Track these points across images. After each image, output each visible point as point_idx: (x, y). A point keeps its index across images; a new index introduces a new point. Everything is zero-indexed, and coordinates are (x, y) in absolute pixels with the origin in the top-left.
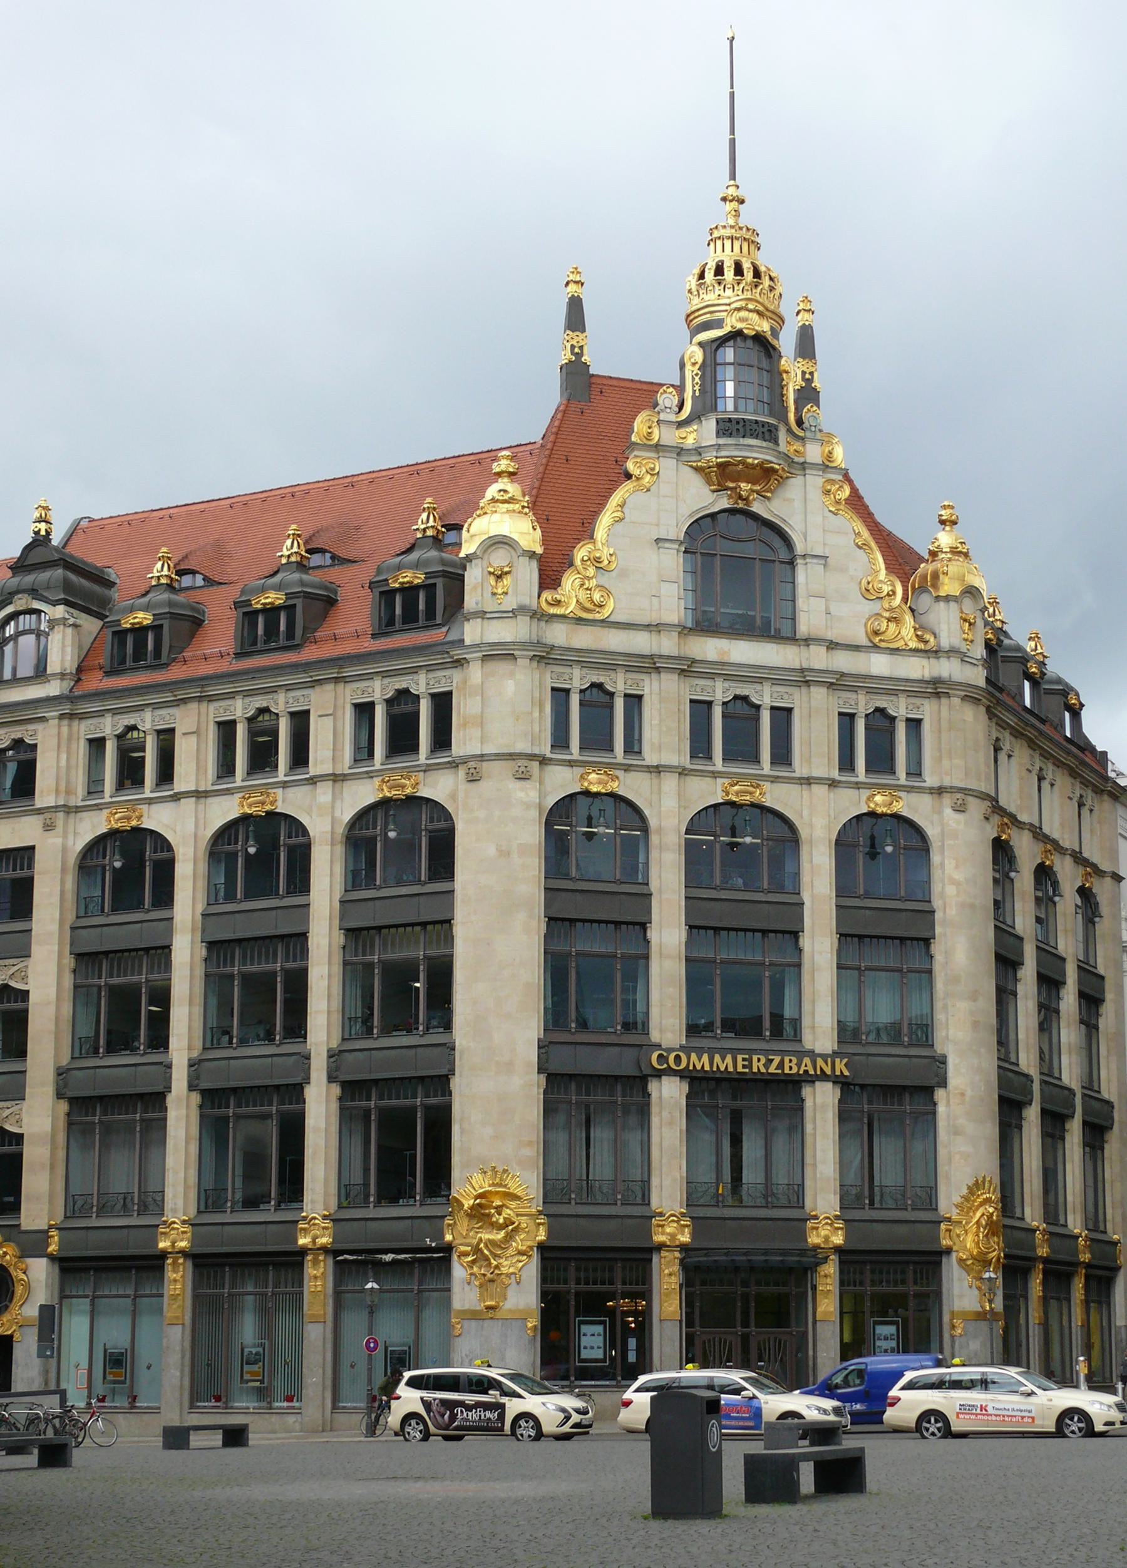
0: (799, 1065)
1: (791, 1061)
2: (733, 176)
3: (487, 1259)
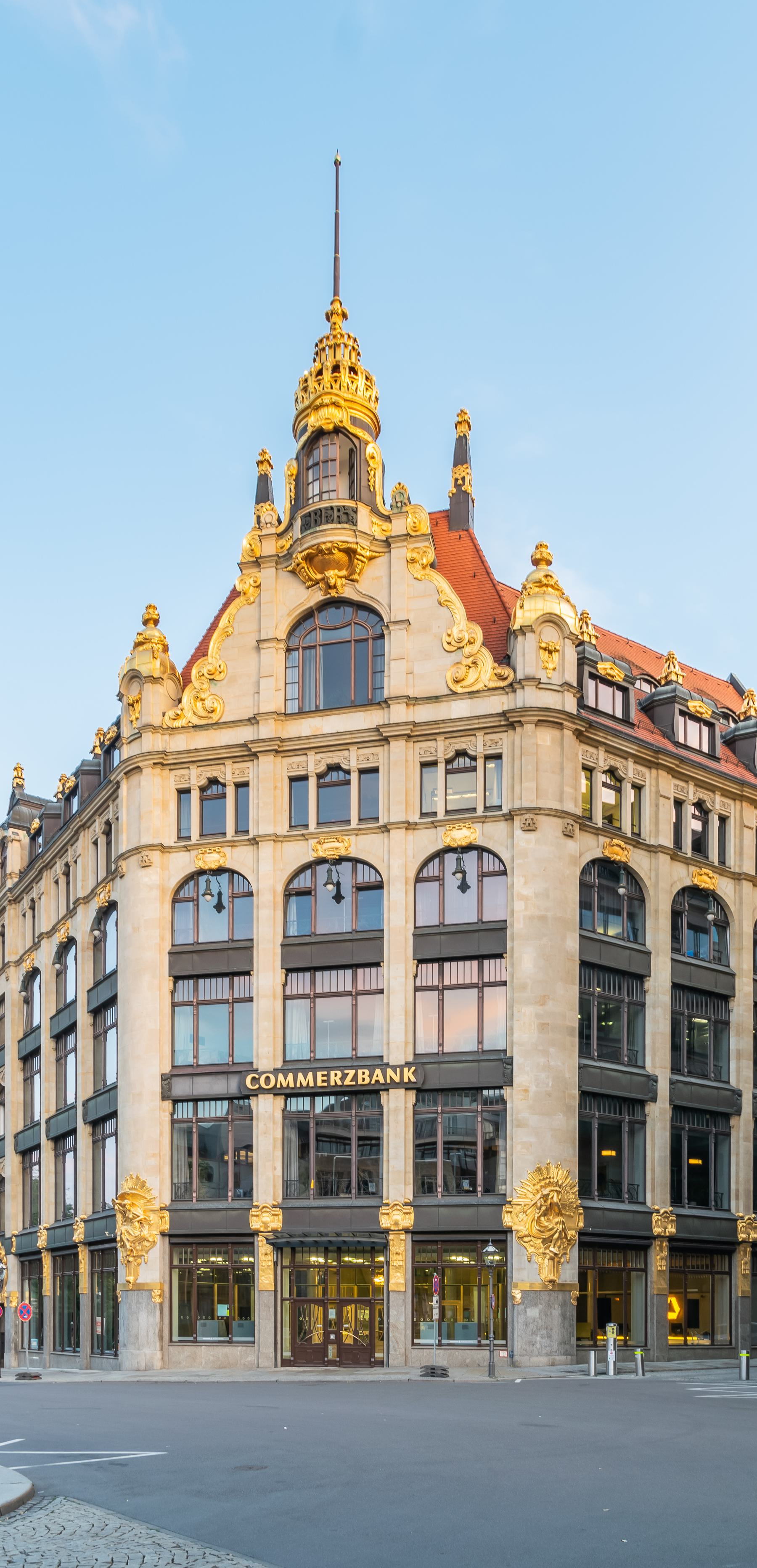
0: (371, 1076)
1: (364, 1073)
2: (336, 293)
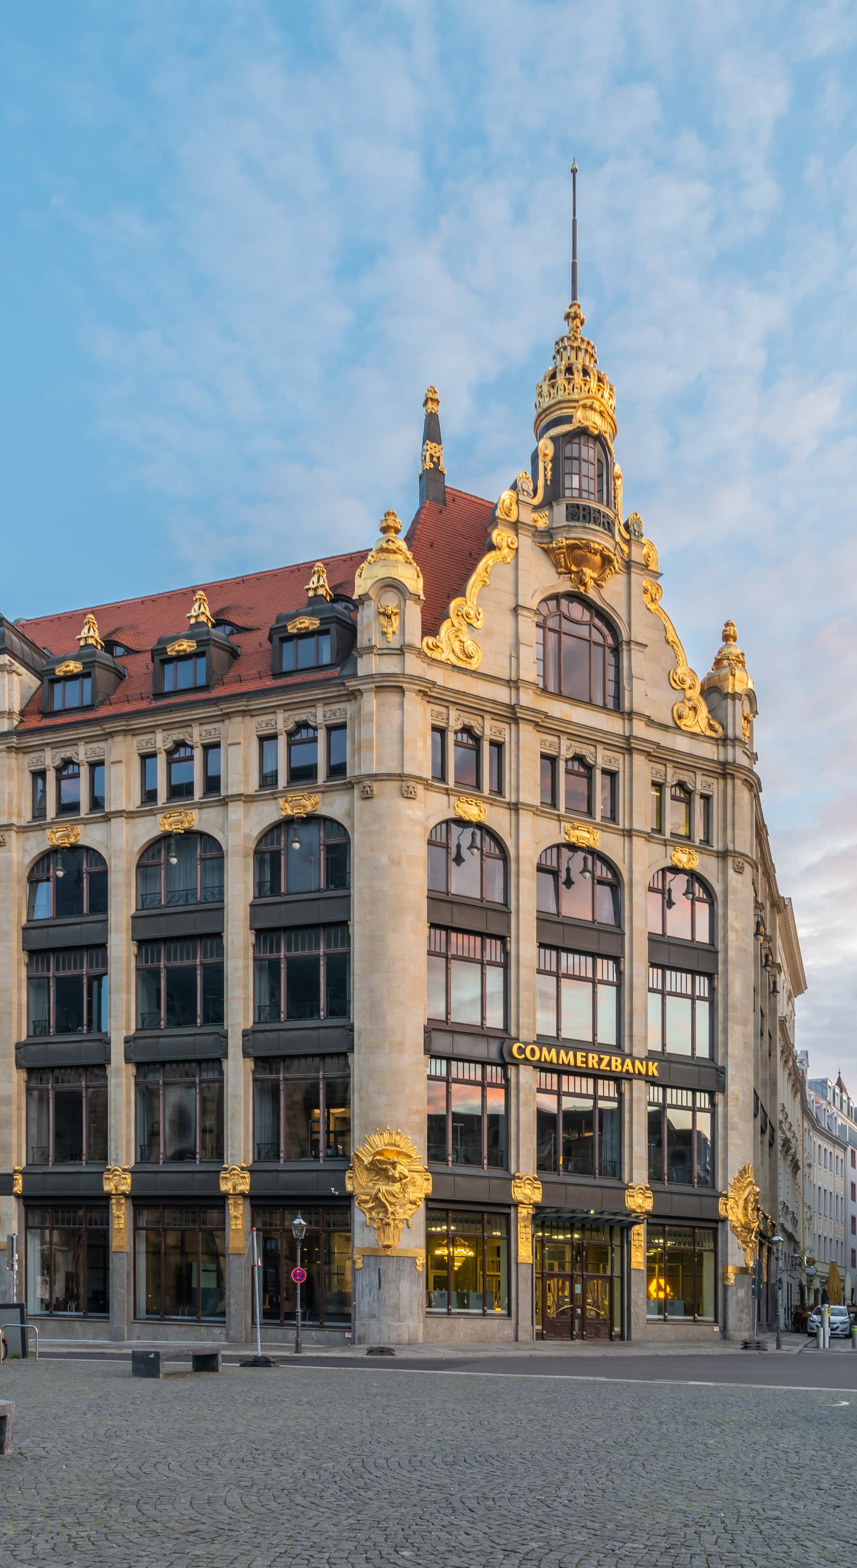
0: (622, 1064)
1: (616, 1061)
3: (384, 1206)
